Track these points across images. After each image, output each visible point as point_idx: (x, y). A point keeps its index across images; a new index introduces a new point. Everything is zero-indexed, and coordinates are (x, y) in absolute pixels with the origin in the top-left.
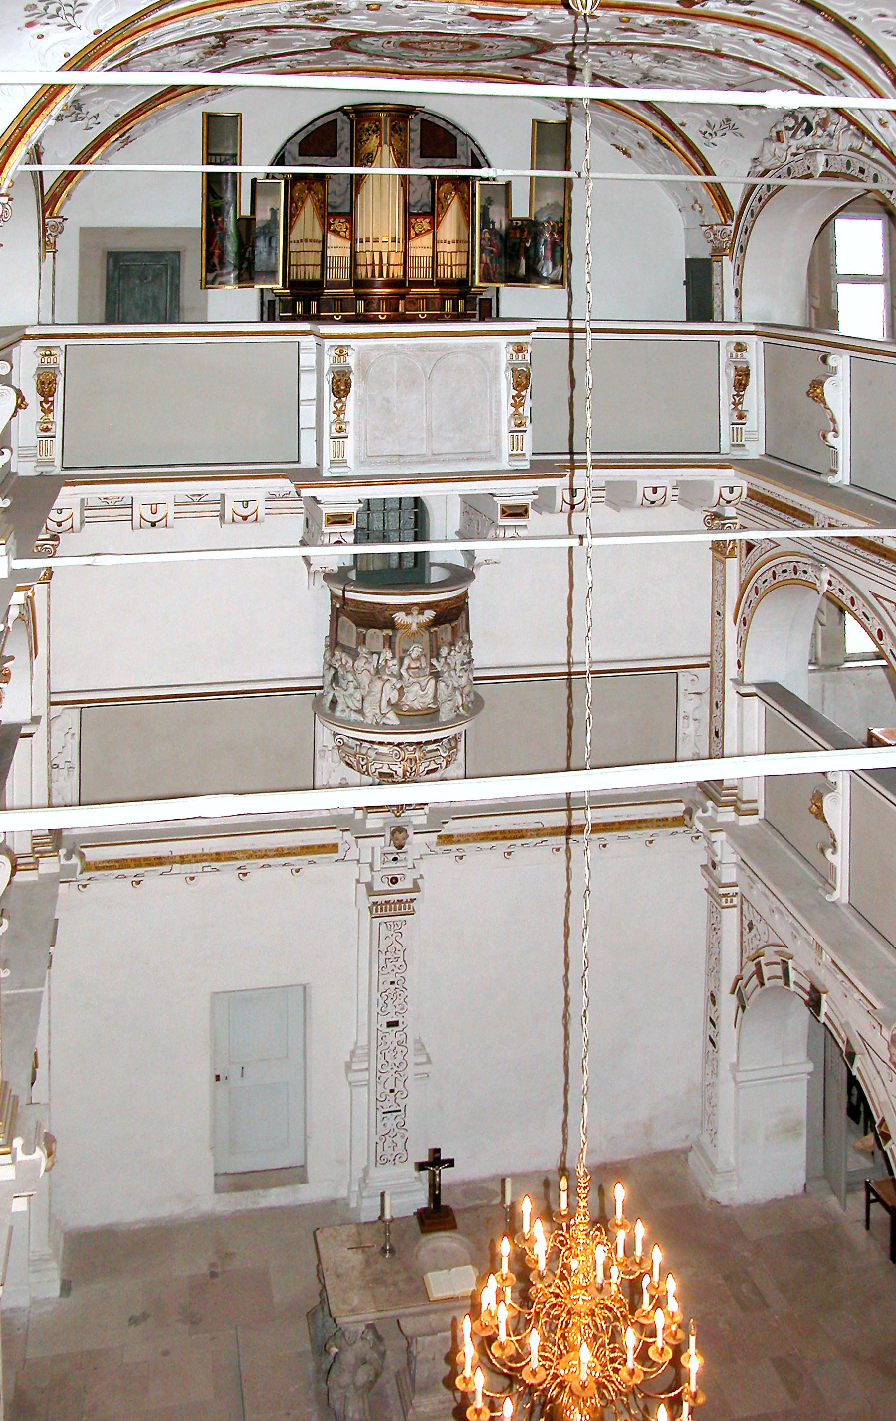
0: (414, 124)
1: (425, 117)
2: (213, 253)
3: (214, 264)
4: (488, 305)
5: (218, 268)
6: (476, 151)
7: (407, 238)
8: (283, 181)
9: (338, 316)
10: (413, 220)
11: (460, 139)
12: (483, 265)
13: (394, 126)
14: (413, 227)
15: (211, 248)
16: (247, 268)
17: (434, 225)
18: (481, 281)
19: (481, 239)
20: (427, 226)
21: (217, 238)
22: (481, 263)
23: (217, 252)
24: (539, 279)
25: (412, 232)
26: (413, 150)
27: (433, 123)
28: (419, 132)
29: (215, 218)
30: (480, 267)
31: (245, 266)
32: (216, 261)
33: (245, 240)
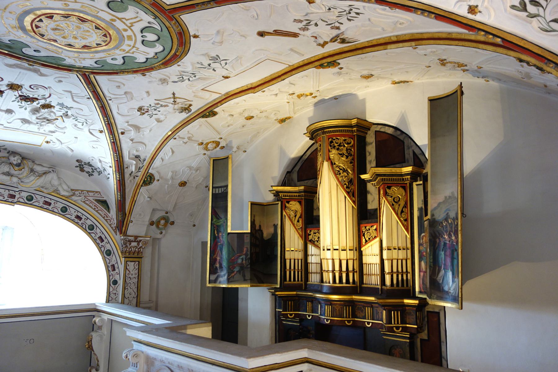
0: (371, 138)
1: (378, 128)
2: (216, 260)
3: (216, 267)
4: (436, 319)
5: (219, 271)
6: (417, 151)
7: (360, 245)
8: (280, 203)
9: (309, 316)
10: (364, 229)
11: (406, 142)
12: (422, 274)
13: (332, 142)
14: (364, 235)
15: (215, 256)
16: (239, 272)
17: (378, 231)
18: (420, 292)
19: (420, 245)
20: (374, 234)
21: (219, 248)
22: (420, 271)
23: (218, 258)
24: (439, 294)
25: (364, 240)
26: (370, 162)
27: (384, 132)
28: (374, 144)
29: (218, 233)
30: (420, 275)
31: (237, 269)
32: (218, 265)
33: (235, 249)
